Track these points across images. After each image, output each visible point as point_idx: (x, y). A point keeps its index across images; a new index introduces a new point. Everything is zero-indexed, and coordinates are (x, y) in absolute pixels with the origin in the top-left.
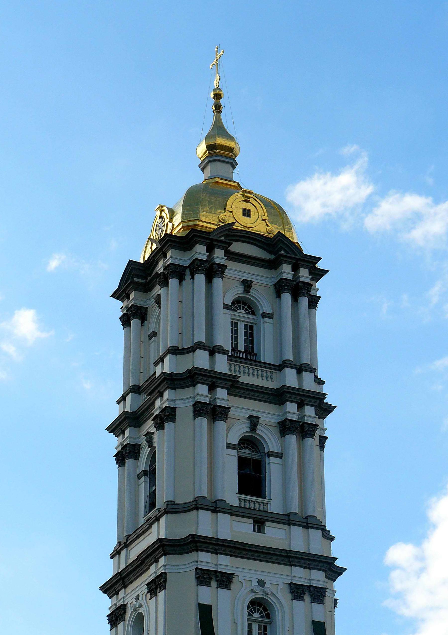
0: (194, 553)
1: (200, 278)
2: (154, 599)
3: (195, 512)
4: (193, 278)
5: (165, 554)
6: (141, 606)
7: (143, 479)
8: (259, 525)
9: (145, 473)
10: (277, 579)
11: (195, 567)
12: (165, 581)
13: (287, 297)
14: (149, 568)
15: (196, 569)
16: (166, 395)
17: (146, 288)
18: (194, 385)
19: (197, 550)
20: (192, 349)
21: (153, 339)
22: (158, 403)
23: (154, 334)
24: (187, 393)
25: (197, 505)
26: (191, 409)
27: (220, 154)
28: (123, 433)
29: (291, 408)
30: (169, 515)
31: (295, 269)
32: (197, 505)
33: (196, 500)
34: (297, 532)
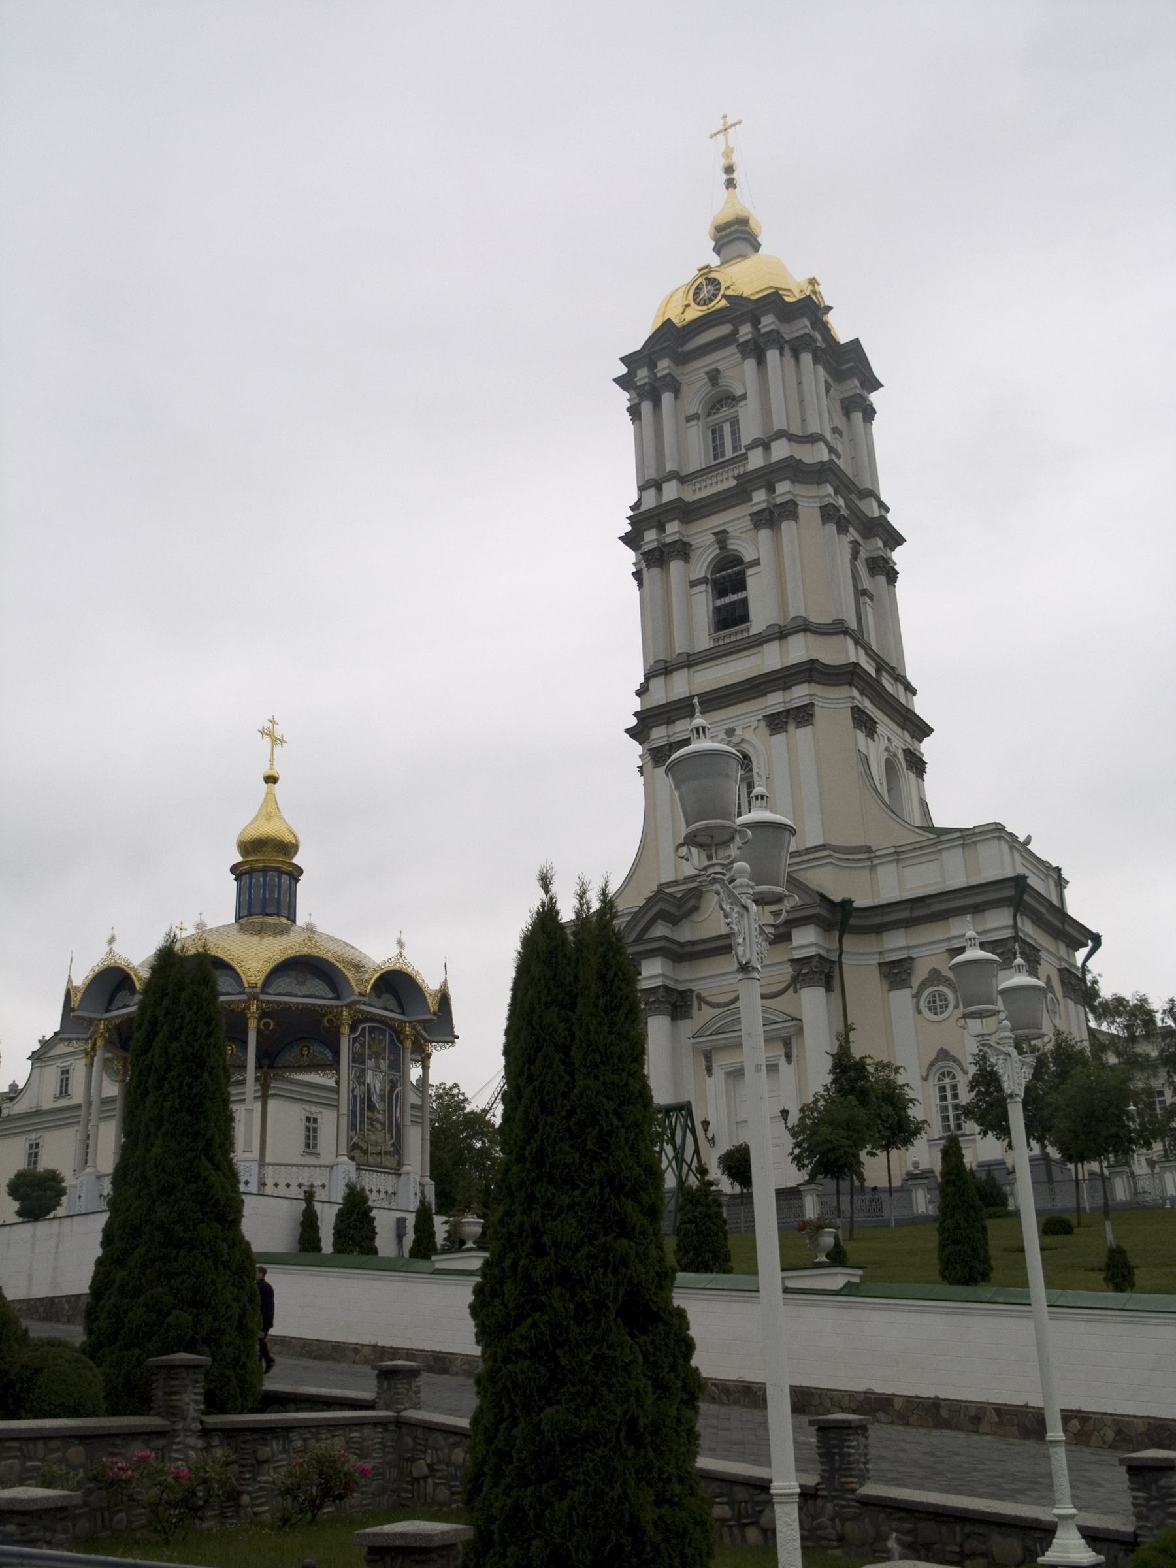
0: (847, 687)
1: (807, 358)
2: (780, 738)
3: (842, 636)
4: (796, 357)
5: (809, 682)
6: (743, 740)
7: (703, 587)
8: (878, 670)
9: (704, 581)
10: (900, 739)
11: (850, 705)
12: (812, 715)
13: (858, 416)
14: (765, 695)
15: (852, 708)
16: (783, 488)
17: (683, 359)
18: (819, 483)
19: (851, 684)
20: (813, 439)
21: (695, 422)
22: (759, 497)
23: (696, 417)
24: (811, 490)
25: (838, 629)
26: (817, 514)
27: (735, 236)
28: (661, 528)
29: (880, 544)
30: (809, 635)
31: (863, 386)
32: (838, 629)
33: (835, 622)
34: (901, 688)
